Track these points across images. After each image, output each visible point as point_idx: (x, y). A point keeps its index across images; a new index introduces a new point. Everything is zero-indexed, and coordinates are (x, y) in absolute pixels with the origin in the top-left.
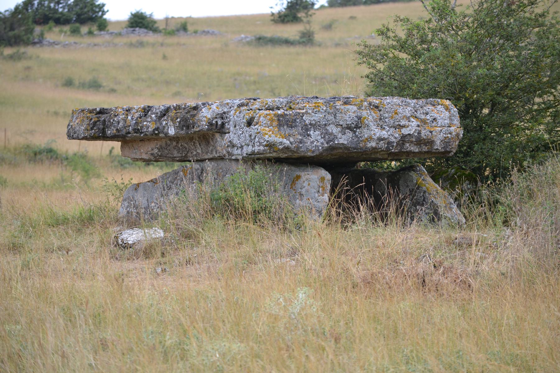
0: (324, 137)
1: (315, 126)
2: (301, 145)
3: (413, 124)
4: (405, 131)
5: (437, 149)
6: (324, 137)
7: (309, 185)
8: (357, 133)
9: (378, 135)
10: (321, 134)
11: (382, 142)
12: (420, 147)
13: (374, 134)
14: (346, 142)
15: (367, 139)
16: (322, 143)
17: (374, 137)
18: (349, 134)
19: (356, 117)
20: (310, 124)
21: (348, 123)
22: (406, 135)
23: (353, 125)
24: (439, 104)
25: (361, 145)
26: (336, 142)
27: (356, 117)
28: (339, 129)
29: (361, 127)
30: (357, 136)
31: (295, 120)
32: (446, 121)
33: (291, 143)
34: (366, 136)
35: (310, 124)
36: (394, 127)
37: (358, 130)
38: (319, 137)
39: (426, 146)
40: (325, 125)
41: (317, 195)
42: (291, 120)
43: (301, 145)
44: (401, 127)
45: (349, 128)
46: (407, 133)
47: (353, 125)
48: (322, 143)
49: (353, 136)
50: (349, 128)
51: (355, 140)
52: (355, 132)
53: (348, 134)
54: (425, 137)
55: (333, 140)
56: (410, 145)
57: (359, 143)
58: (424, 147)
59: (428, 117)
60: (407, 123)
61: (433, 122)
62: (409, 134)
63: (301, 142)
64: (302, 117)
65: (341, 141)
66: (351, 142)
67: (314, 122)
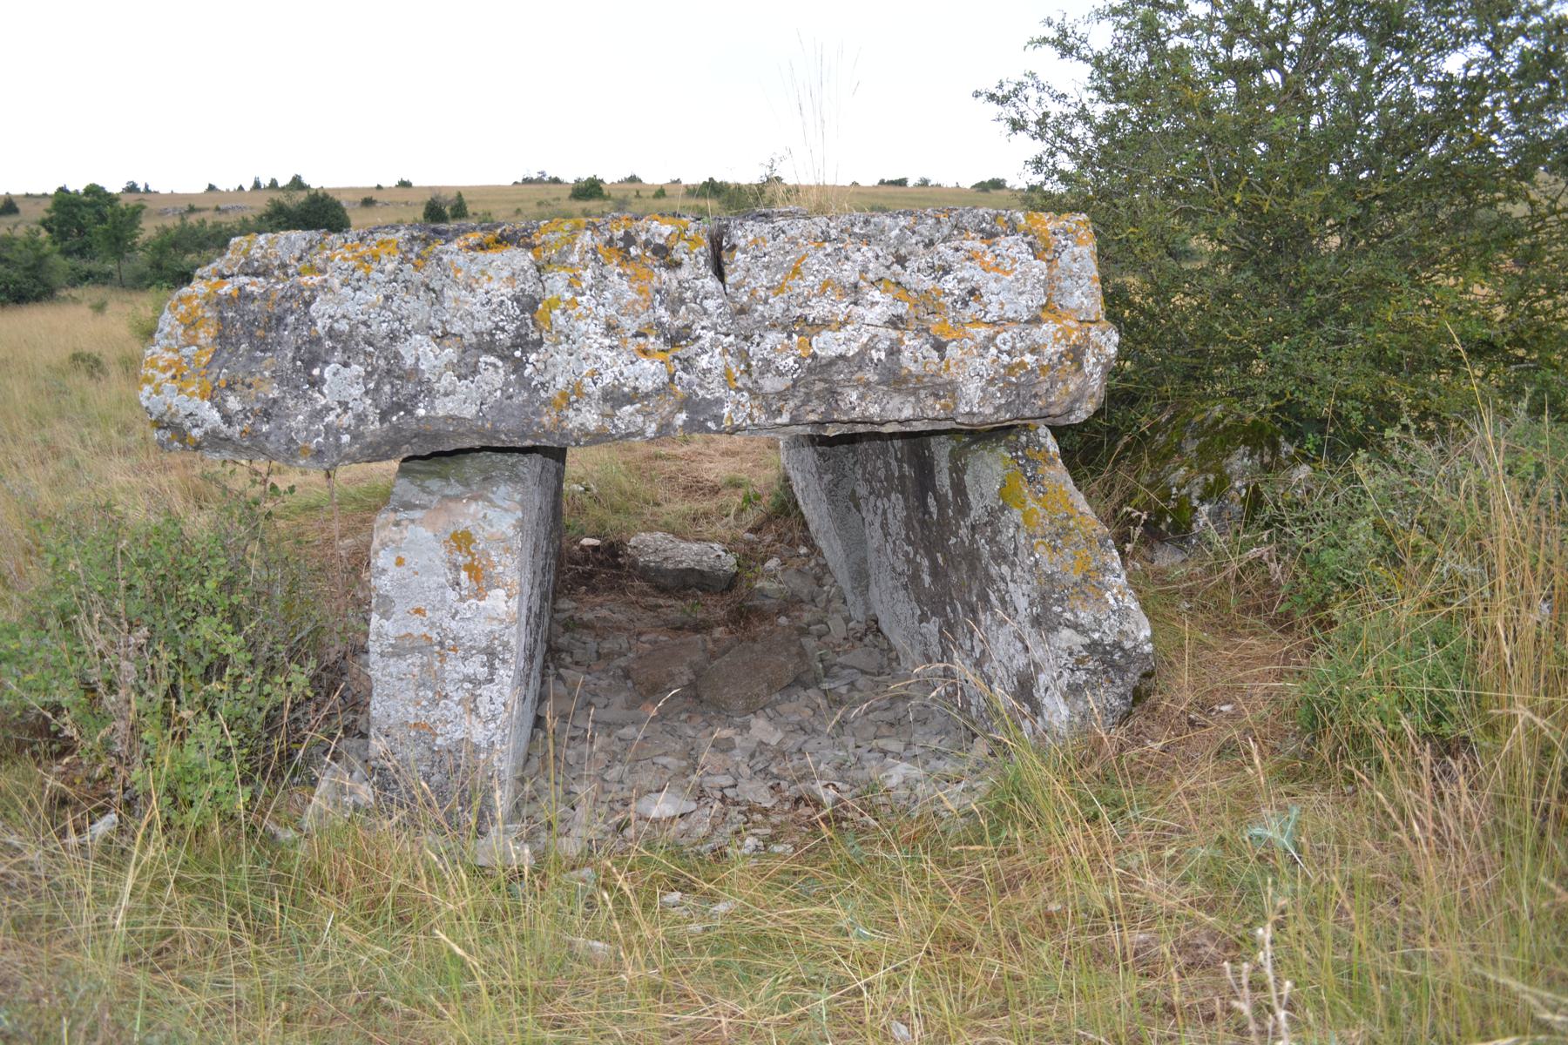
0: (377, 389)
1: (346, 343)
2: (265, 428)
3: (872, 315)
4: (827, 344)
5: (971, 414)
6: (377, 389)
7: (400, 562)
8: (529, 370)
9: (608, 379)
10: (369, 375)
11: (628, 409)
12: (918, 400)
13: (593, 373)
14: (469, 411)
15: (564, 396)
16: (361, 418)
17: (591, 389)
18: (493, 374)
19: (516, 299)
20: (331, 333)
21: (478, 326)
22: (832, 362)
23: (500, 336)
24: (1014, 231)
25: (545, 420)
26: (421, 412)
27: (516, 299)
28: (450, 353)
29: (540, 343)
30: (525, 383)
31: (280, 320)
32: (1023, 300)
33: (227, 418)
34: (561, 382)
35: (331, 333)
36: (785, 328)
37: (533, 357)
38: (357, 391)
39: (937, 397)
40: (393, 337)
41: (452, 595)
42: (263, 319)
43: (265, 428)
44: (808, 326)
45: (488, 345)
46: (833, 352)
47: (500, 336)
48: (361, 418)
49: (507, 384)
50: (488, 345)
51: (517, 401)
52: (519, 366)
53: (489, 374)
54: (913, 368)
55: (407, 406)
56: (862, 397)
57: (537, 413)
58: (930, 401)
59: (949, 283)
60: (842, 309)
61: (966, 304)
62: (842, 357)
63: (267, 415)
64: (308, 304)
65: (445, 407)
66: (499, 408)
67: (343, 326)
